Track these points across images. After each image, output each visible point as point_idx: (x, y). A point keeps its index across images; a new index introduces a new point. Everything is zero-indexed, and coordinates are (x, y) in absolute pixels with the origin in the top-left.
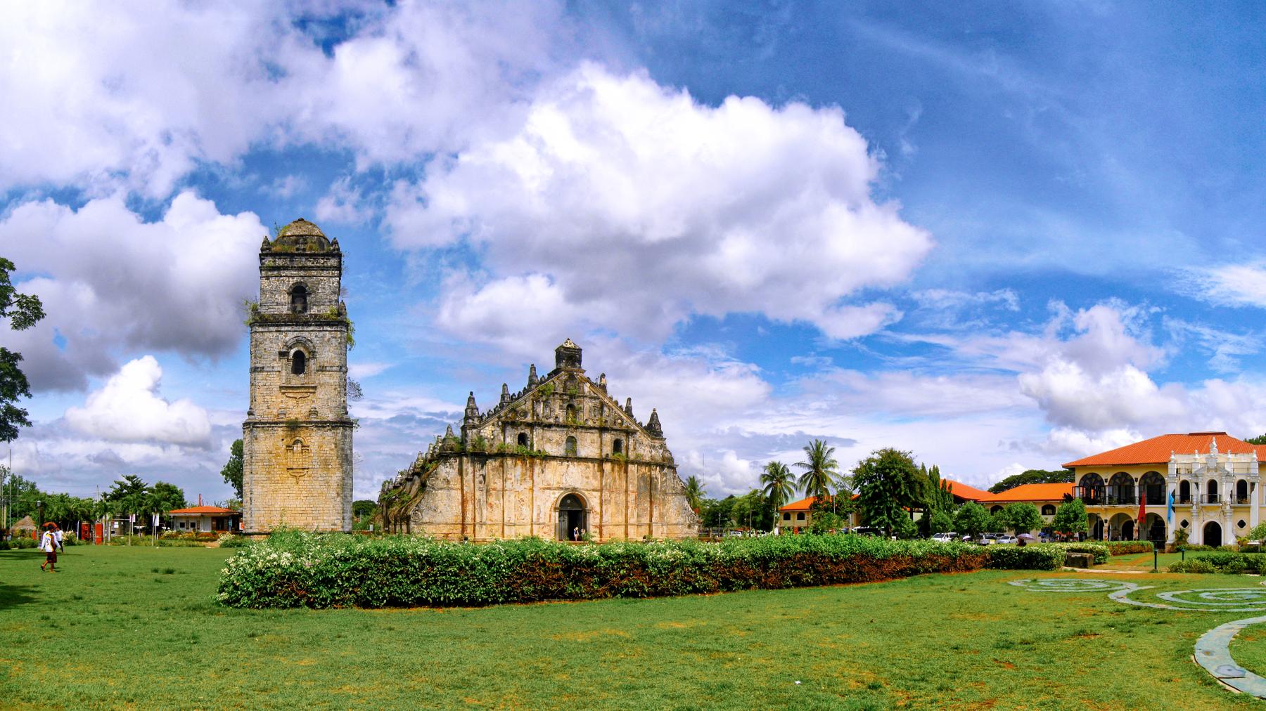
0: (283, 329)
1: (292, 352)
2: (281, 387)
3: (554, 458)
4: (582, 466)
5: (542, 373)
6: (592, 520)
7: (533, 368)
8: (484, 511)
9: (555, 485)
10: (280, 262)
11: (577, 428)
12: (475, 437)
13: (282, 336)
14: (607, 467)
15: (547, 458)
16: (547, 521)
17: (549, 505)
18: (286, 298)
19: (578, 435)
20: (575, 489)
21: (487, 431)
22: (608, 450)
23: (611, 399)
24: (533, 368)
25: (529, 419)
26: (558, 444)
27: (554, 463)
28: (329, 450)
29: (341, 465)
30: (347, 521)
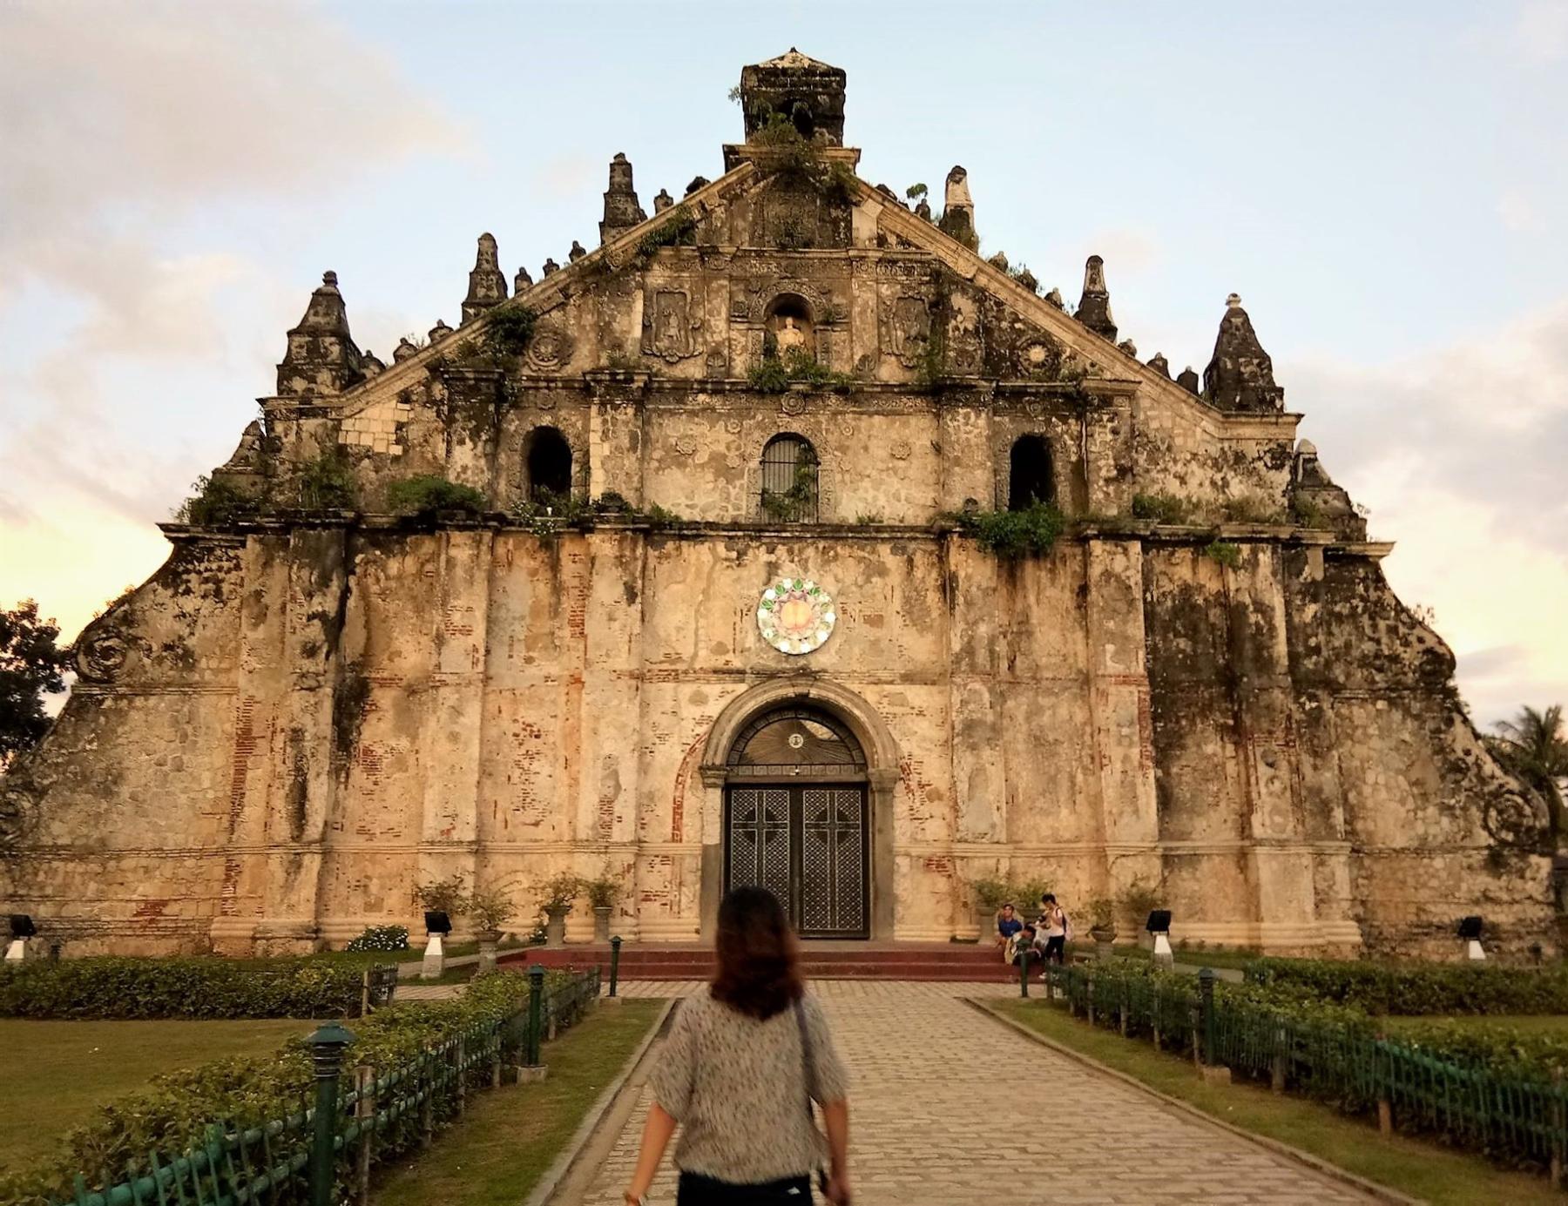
3: (694, 532)
4: (848, 565)
5: (662, 178)
6: (910, 828)
7: (621, 167)
8: (319, 789)
9: (706, 659)
11: (815, 393)
12: (312, 451)
15: (657, 529)
17: (670, 755)
19: (823, 424)
20: (806, 673)
21: (373, 424)
22: (979, 483)
23: (999, 264)
24: (621, 167)
25: (583, 360)
26: (722, 469)
27: (699, 555)
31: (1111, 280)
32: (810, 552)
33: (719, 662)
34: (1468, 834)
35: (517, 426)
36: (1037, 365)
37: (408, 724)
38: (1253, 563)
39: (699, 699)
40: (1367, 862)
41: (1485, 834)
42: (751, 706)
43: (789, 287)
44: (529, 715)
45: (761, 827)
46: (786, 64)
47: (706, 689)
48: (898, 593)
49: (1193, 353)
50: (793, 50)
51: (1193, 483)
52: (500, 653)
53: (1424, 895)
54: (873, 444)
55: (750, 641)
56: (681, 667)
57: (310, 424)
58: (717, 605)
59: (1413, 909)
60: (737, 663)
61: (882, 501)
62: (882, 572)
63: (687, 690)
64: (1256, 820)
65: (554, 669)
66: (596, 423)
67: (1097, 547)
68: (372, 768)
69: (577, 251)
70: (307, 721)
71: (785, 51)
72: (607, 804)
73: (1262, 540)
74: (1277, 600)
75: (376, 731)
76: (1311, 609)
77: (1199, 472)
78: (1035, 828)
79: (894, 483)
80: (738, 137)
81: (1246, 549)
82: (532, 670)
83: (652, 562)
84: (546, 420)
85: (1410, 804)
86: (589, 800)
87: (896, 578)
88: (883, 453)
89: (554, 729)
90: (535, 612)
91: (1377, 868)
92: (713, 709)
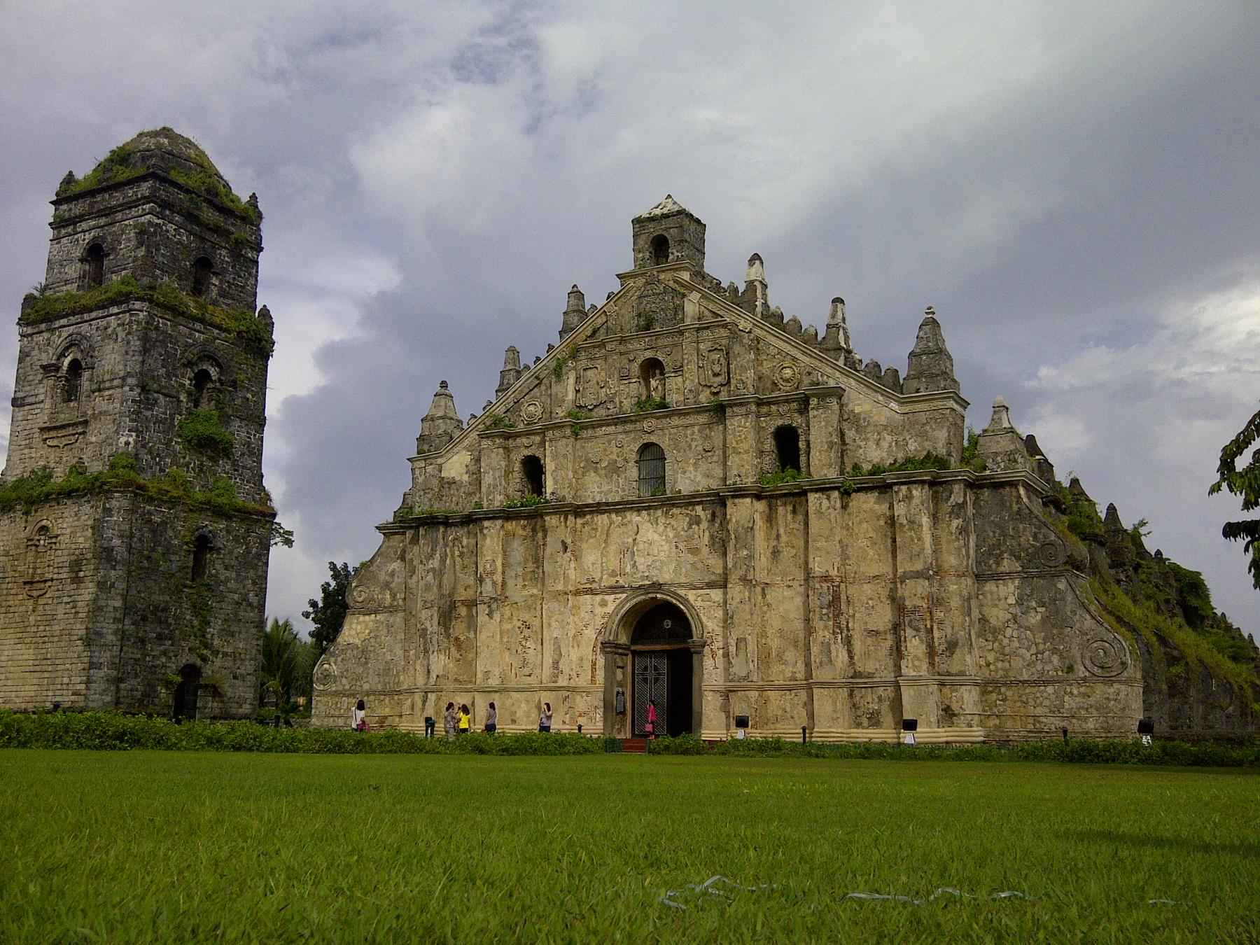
0: (57, 324)
1: (67, 362)
2: (42, 429)
3: (599, 508)
4: (680, 519)
9: (608, 581)
10: (77, 208)
13: (55, 338)
14: (743, 511)
15: (579, 511)
16: (583, 681)
17: (590, 634)
18: (74, 270)
20: (657, 586)
21: (456, 465)
26: (614, 469)
27: (602, 520)
28: (84, 540)
29: (96, 569)
30: (98, 686)
31: (849, 309)
32: (659, 512)
33: (612, 582)
34: (1070, 669)
35: (518, 457)
36: (787, 381)
37: (472, 625)
38: (909, 497)
39: (604, 604)
40: (1003, 690)
41: (1082, 668)
42: (628, 606)
43: (649, 354)
44: (526, 616)
45: (651, 675)
46: (658, 212)
47: (607, 597)
48: (707, 534)
49: (895, 353)
50: (669, 196)
51: (885, 444)
52: (510, 583)
53: (1039, 711)
54: (694, 444)
55: (628, 569)
56: (594, 586)
57: (429, 469)
58: (613, 548)
59: (1031, 720)
60: (621, 582)
61: (699, 478)
62: (698, 524)
63: (598, 598)
64: (903, 663)
65: (535, 591)
66: (548, 452)
67: (812, 497)
68: (459, 648)
69: (551, 347)
70: (428, 624)
71: (661, 199)
72: (556, 664)
73: (914, 482)
74: (925, 520)
75: (458, 629)
76: (955, 523)
77: (889, 438)
78: (782, 672)
79: (703, 466)
80: (628, 266)
81: (904, 488)
82: (525, 593)
83: (579, 526)
84: (527, 452)
85: (1033, 650)
86: (548, 660)
87: (704, 525)
88: (700, 448)
89: (536, 622)
90: (526, 561)
91: (1009, 693)
92: (610, 608)
